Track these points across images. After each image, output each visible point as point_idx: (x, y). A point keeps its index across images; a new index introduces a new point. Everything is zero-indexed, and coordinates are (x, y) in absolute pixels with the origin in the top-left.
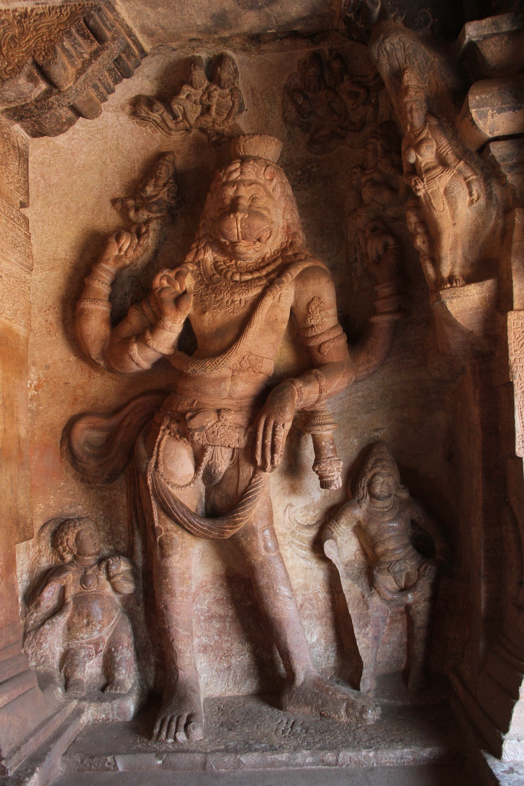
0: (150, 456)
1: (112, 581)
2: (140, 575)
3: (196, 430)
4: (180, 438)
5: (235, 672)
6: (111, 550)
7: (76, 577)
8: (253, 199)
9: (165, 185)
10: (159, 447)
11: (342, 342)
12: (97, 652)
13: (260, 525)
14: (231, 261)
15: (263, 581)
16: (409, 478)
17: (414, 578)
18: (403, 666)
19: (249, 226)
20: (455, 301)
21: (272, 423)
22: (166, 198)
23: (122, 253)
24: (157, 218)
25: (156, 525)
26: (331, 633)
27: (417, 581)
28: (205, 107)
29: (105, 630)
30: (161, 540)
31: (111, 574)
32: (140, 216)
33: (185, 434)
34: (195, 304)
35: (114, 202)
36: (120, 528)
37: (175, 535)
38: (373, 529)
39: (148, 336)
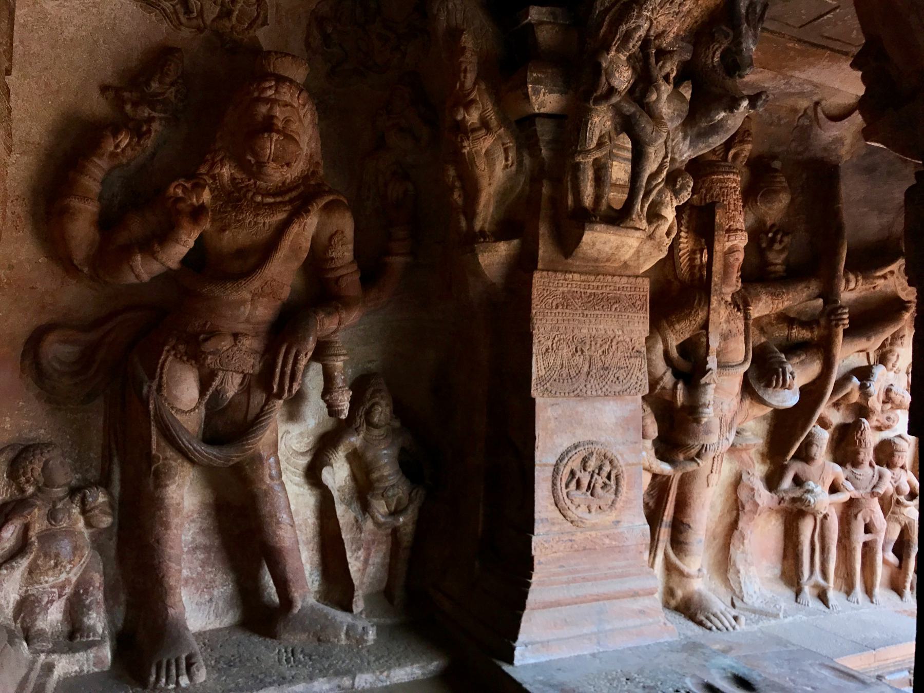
0: (152, 378)
1: (88, 515)
2: (117, 506)
3: (210, 353)
4: (188, 360)
5: (217, 603)
6: (78, 480)
7: (42, 512)
8: (287, 121)
9: (172, 84)
10: (162, 368)
11: (357, 277)
12: (60, 596)
13: (265, 454)
14: (249, 180)
15: (266, 510)
16: (399, 410)
17: (405, 501)
18: (384, 585)
19: (284, 148)
20: (486, 255)
21: (294, 351)
22: (173, 99)
23: (119, 150)
24: (161, 119)
25: (154, 452)
26: (316, 558)
27: (408, 505)
28: (224, 9)
29: (75, 570)
30: (157, 469)
31: (88, 507)
32: (139, 112)
33: (195, 356)
34: (213, 221)
35: (104, 89)
36: (92, 455)
37: (174, 464)
38: (369, 455)
39: (157, 247)
